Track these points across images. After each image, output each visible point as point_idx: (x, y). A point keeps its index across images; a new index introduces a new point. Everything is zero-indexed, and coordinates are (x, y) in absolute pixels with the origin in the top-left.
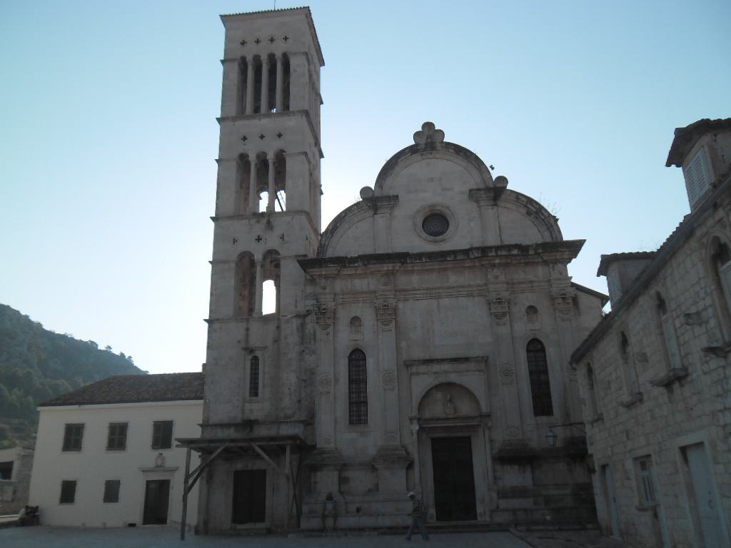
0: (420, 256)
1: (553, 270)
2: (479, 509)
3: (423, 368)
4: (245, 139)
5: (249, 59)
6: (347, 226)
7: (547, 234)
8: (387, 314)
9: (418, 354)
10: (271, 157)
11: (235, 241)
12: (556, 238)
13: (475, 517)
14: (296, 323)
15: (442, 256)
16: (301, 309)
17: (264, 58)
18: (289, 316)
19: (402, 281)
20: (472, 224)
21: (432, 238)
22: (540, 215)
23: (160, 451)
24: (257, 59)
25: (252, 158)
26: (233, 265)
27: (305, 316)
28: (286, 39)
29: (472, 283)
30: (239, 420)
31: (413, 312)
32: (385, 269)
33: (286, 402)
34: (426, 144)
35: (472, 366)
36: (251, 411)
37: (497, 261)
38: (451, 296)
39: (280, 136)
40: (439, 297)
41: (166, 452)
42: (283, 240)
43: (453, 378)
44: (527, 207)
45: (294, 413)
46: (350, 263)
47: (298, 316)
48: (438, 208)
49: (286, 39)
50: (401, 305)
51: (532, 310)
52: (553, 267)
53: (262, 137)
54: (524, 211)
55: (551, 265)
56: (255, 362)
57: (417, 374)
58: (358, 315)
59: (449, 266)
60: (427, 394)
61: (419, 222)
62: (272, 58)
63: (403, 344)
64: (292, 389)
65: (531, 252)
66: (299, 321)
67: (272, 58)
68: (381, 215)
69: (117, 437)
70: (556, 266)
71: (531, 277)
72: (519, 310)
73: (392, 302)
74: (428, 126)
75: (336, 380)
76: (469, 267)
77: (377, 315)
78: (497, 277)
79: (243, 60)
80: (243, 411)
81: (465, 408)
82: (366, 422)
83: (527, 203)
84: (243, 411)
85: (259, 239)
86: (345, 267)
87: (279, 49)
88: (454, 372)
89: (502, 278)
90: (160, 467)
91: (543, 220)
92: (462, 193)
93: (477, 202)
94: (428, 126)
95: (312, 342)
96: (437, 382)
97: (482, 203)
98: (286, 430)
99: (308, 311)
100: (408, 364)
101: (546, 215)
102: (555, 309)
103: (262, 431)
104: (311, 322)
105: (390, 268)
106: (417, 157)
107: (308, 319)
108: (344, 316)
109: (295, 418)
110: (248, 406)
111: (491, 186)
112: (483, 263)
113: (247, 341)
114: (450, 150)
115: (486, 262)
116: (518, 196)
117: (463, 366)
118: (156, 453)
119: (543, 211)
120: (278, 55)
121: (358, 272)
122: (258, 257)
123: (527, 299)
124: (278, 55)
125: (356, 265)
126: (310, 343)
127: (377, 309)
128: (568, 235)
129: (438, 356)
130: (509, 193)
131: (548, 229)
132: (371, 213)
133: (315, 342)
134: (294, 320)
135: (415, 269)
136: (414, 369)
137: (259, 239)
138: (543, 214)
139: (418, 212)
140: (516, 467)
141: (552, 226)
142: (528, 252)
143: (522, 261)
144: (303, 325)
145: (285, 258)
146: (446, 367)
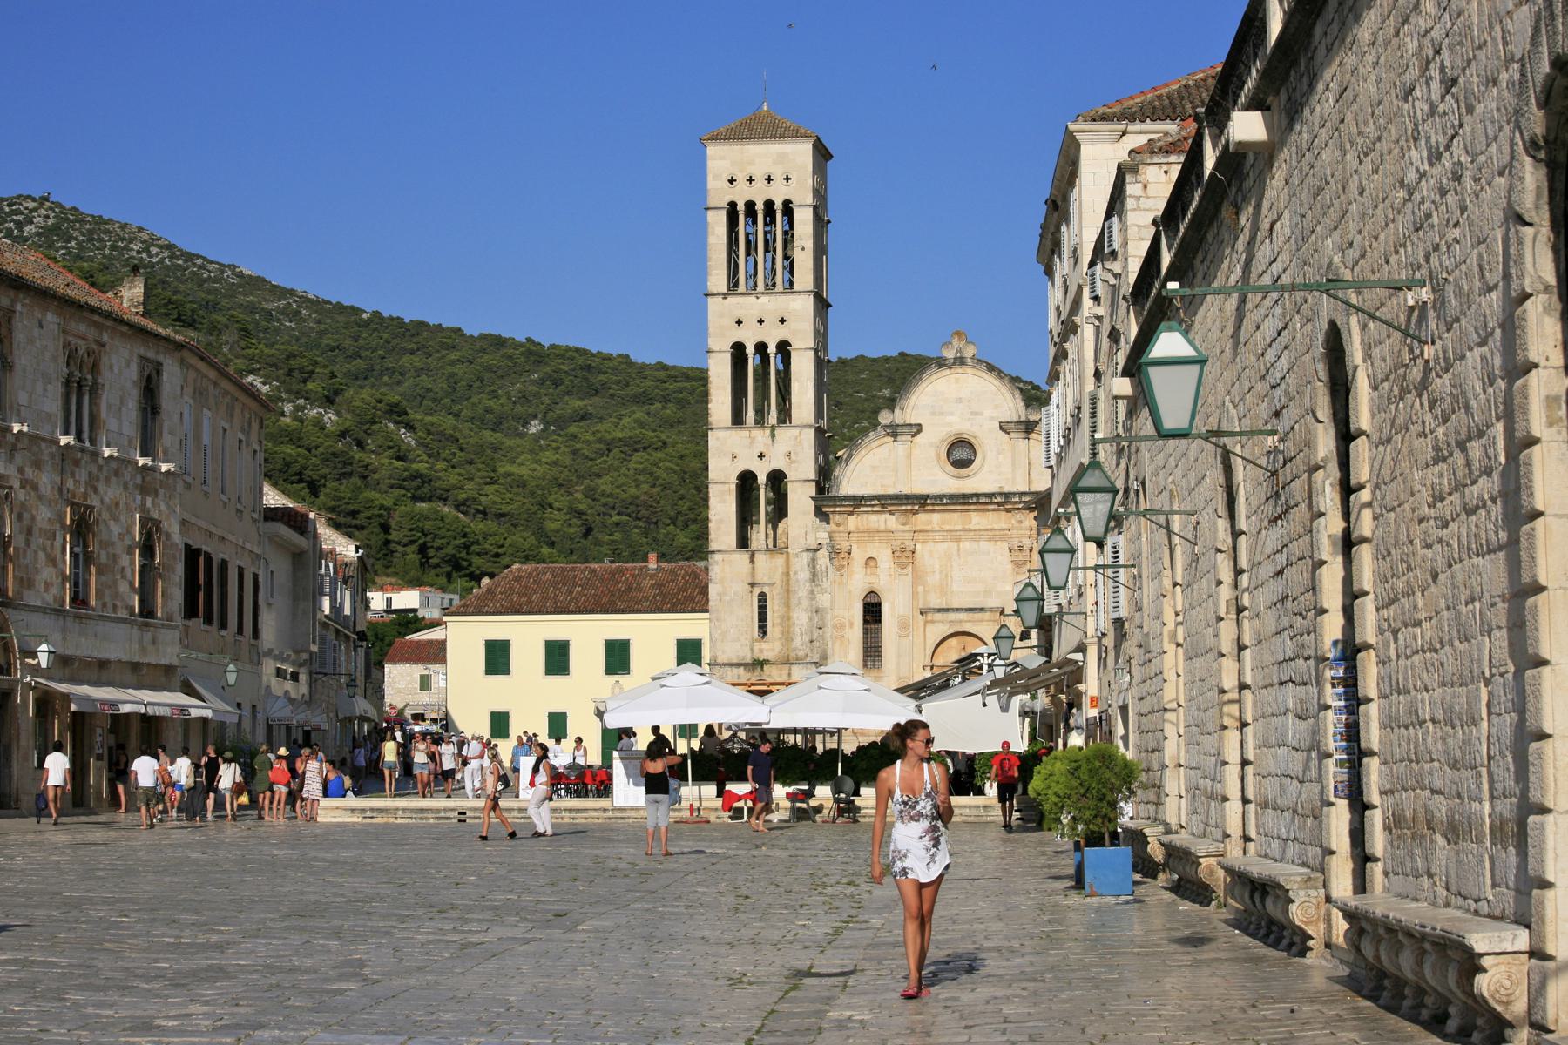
3: (938, 616)
4: (739, 322)
6: (863, 452)
8: (905, 556)
9: (936, 602)
11: (734, 457)
14: (806, 557)
19: (922, 518)
20: (1001, 457)
23: (616, 677)
28: (787, 179)
29: (996, 527)
30: (749, 660)
31: (930, 554)
33: (798, 642)
34: (955, 359)
35: (987, 615)
36: (761, 651)
38: (973, 540)
39: (782, 321)
40: (958, 540)
43: (968, 628)
49: (787, 179)
50: (919, 547)
53: (761, 322)
57: (932, 622)
62: (769, 205)
63: (920, 589)
66: (810, 554)
69: (557, 658)
73: (909, 545)
75: (851, 625)
78: (1021, 522)
79: (732, 206)
80: (752, 650)
84: (752, 650)
92: (992, 419)
96: (952, 631)
108: (858, 555)
109: (808, 660)
110: (757, 646)
122: (762, 479)
129: (956, 606)
136: (930, 617)
137: (761, 456)
139: (943, 441)
144: (813, 561)
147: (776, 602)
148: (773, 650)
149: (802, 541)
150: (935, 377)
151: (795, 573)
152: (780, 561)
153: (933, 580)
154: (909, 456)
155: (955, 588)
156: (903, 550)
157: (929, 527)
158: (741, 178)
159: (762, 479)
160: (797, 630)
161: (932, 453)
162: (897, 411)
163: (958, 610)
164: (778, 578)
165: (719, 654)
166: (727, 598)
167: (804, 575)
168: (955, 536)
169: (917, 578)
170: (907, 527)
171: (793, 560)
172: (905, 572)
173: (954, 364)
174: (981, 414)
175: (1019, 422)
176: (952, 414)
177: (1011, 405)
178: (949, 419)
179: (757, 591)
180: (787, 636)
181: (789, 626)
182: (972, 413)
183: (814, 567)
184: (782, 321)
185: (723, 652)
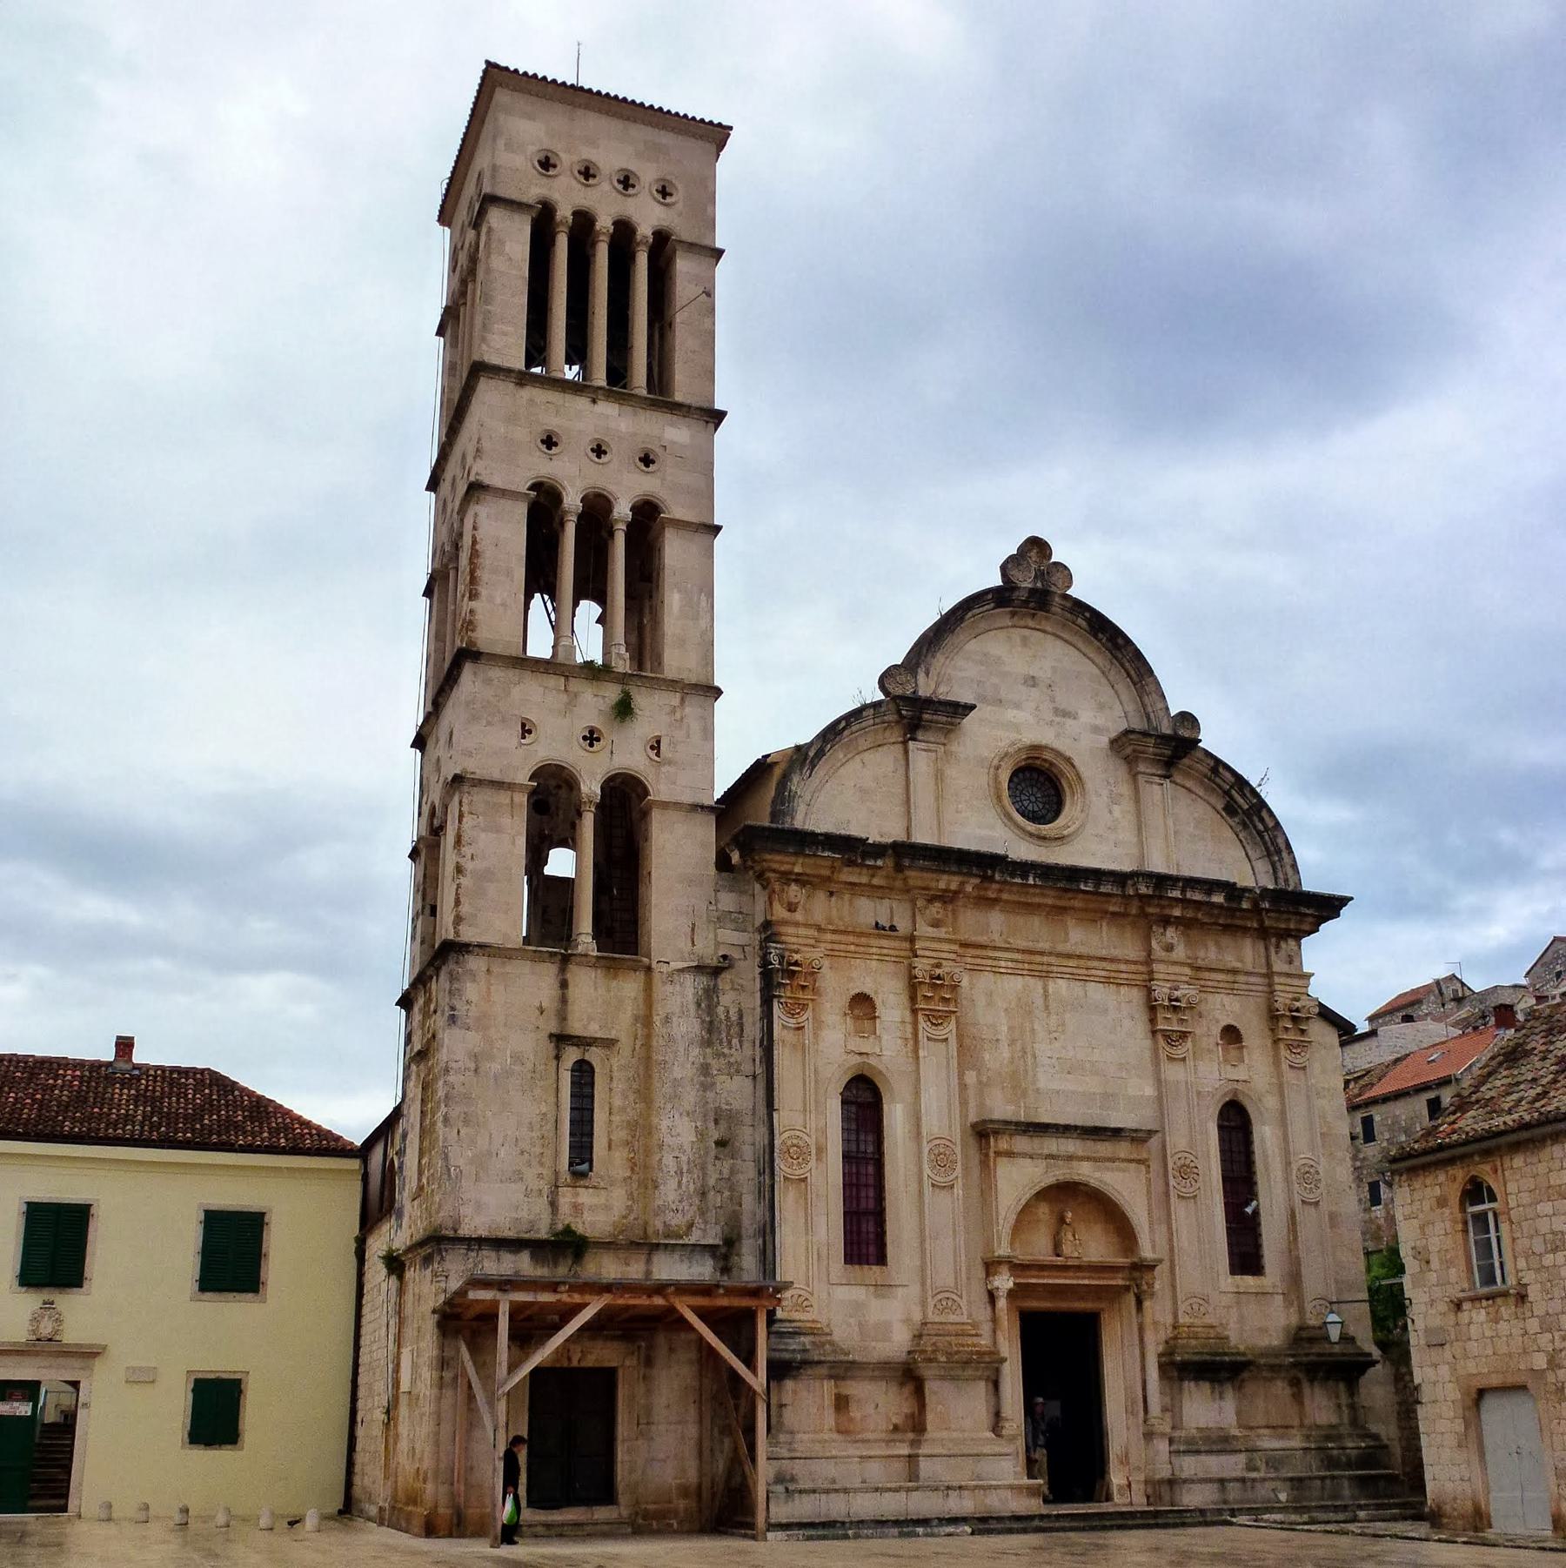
0: (1024, 868)
1: (1277, 953)
2: (1116, 1478)
3: (1022, 1143)
4: (549, 442)
5: (564, 213)
7: (1263, 867)
9: (1001, 1108)
10: (622, 510)
12: (1286, 880)
13: (1109, 1498)
14: (690, 987)
15: (1050, 873)
16: (707, 950)
17: (604, 223)
18: (676, 965)
20: (1117, 810)
21: (1031, 827)
22: (1256, 819)
24: (583, 222)
25: (572, 501)
26: (522, 799)
27: (716, 972)
30: (543, 1234)
32: (942, 885)
33: (669, 1192)
34: (1033, 591)
35: (1123, 1149)
36: (577, 1208)
37: (1177, 912)
38: (1074, 977)
40: (1045, 975)
41: (69, 1303)
42: (658, 755)
43: (1085, 1172)
44: (1231, 797)
45: (691, 1226)
46: (865, 855)
47: (699, 969)
48: (1047, 756)
49: (664, 192)
51: (1231, 1035)
52: (1278, 946)
53: (599, 451)
54: (1220, 806)
55: (1273, 940)
56: (583, 1075)
57: (1010, 1154)
58: (867, 991)
59: (1077, 904)
60: (1026, 1211)
61: (1005, 776)
63: (971, 1077)
64: (684, 1158)
65: (1245, 905)
66: (703, 981)
67: (624, 231)
68: (923, 745)
70: (1283, 945)
71: (1230, 960)
72: (1207, 1032)
74: (1036, 547)
75: (821, 1150)
76: (1114, 914)
77: (913, 999)
78: (1169, 948)
80: (553, 1205)
81: (1092, 1245)
82: (881, 1260)
83: (1232, 787)
84: (553, 1205)
85: (592, 737)
86: (851, 863)
87: (648, 217)
88: (1088, 1159)
89: (1180, 952)
90: (44, 1346)
91: (1259, 833)
92: (1096, 730)
93: (1130, 761)
94: (1036, 547)
95: (735, 1041)
96: (1050, 1180)
97: (1142, 768)
98: (669, 1269)
99: (725, 957)
100: (983, 1132)
101: (1271, 824)
102: (1276, 1042)
103: (608, 1268)
104: (733, 989)
105: (953, 887)
106: (1002, 616)
107: (724, 981)
108: (836, 985)
109: (694, 1238)
111: (1166, 729)
112: (1151, 910)
113: (562, 1016)
114: (1080, 621)
115: (1157, 910)
116: (1217, 765)
117: (1104, 1148)
118: (31, 1301)
119: (1264, 814)
120: (645, 231)
121: (876, 881)
123: (1224, 1008)
124: (645, 231)
125: (880, 863)
126: (730, 1042)
127: (913, 986)
128: (1313, 881)
130: (1200, 755)
131: (1269, 855)
132: (895, 735)
133: (741, 1042)
134: (689, 979)
135: (1005, 896)
136: (1003, 1144)
138: (1262, 820)
140: (1206, 1386)
141: (1279, 852)
142: (1240, 903)
143: (1221, 921)
145: (665, 805)
146: (1071, 1146)
147: (618, 1086)
148: (607, 1208)
149: (684, 944)
150: (983, 625)
151: (667, 1020)
152: (630, 987)
153: (997, 1058)
154: (939, 776)
155: (1043, 1082)
156: (936, 981)
157: (982, 939)
158: (568, 160)
159: (591, 787)
160: (669, 1161)
161: (983, 779)
162: (921, 676)
163: (1065, 1130)
164: (622, 1027)
165: (466, 1210)
166: (496, 1067)
167: (686, 1027)
168: (1037, 965)
169: (967, 1052)
170: (941, 933)
171: (661, 989)
172: (941, 1032)
173: (1025, 603)
174: (1073, 716)
175: (1164, 739)
176: (1017, 706)
177: (1130, 708)
178: (1011, 714)
179: (572, 1055)
180: (644, 1177)
181: (648, 1152)
182: (1057, 711)
183: (711, 1009)
184: (647, 460)
185: (479, 1206)
